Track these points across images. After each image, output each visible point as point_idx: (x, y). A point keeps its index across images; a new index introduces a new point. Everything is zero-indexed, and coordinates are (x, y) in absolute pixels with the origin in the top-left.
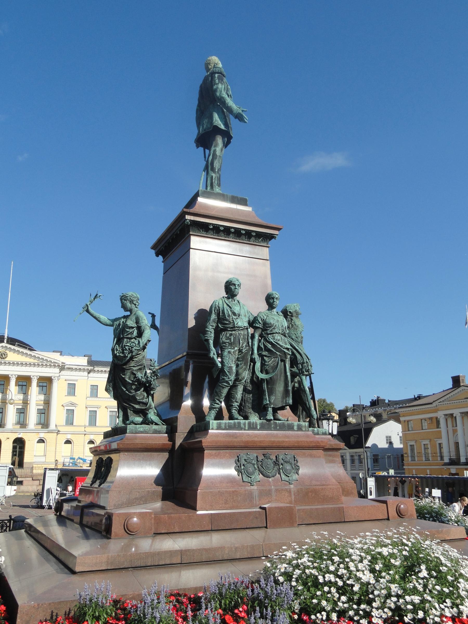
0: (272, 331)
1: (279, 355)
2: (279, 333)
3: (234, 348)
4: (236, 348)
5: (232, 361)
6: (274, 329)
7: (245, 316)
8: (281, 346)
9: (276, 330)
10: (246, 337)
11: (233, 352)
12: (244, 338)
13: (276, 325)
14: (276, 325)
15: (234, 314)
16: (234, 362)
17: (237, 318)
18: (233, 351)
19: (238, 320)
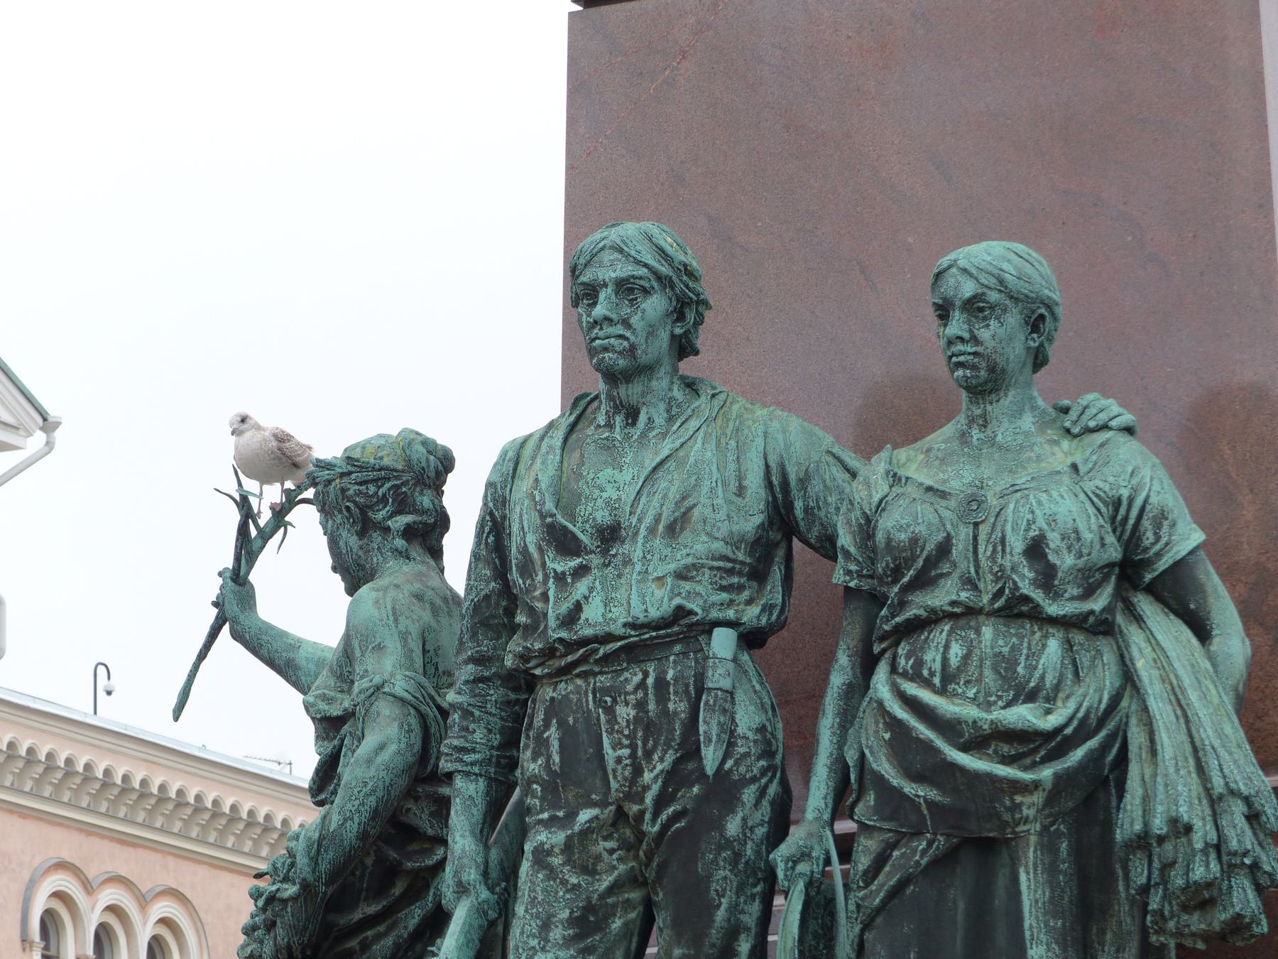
0: (902, 605)
1: (931, 804)
2: (971, 612)
3: (572, 815)
4: (585, 816)
5: (546, 926)
6: (924, 580)
7: (673, 530)
8: (948, 728)
9: (942, 596)
10: (678, 705)
11: (568, 847)
12: (647, 726)
13: (944, 549)
14: (944, 549)
15: (563, 542)
16: (557, 934)
17: (581, 571)
18: (559, 837)
19: (581, 587)
